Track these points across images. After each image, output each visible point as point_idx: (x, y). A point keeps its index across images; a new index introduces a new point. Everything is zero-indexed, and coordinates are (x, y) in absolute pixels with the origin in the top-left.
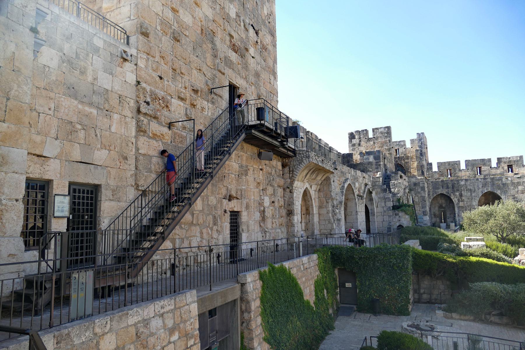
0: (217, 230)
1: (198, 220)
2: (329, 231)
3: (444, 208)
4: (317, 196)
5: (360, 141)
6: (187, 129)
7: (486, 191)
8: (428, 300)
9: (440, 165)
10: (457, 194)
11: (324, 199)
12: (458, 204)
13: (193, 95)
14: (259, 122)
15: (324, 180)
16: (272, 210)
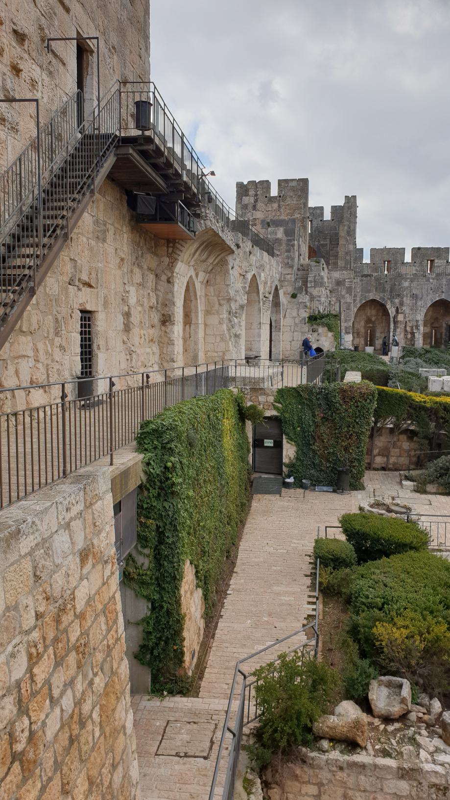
0: (61, 346)
1: (30, 325)
2: (221, 354)
3: (373, 323)
4: (203, 294)
5: (256, 201)
6: (7, 123)
7: (437, 299)
8: (383, 465)
9: (374, 252)
10: (397, 301)
11: (216, 298)
12: (395, 317)
13: (14, 44)
14: (140, 133)
15: (217, 264)
16: (140, 312)
